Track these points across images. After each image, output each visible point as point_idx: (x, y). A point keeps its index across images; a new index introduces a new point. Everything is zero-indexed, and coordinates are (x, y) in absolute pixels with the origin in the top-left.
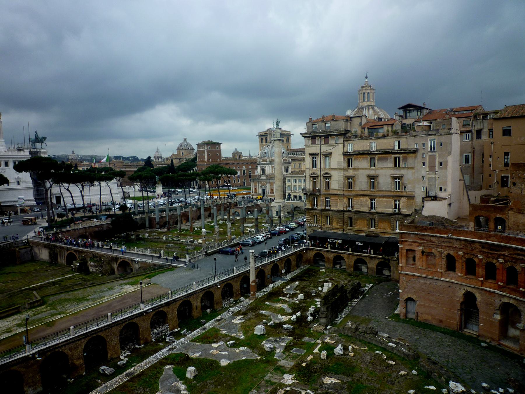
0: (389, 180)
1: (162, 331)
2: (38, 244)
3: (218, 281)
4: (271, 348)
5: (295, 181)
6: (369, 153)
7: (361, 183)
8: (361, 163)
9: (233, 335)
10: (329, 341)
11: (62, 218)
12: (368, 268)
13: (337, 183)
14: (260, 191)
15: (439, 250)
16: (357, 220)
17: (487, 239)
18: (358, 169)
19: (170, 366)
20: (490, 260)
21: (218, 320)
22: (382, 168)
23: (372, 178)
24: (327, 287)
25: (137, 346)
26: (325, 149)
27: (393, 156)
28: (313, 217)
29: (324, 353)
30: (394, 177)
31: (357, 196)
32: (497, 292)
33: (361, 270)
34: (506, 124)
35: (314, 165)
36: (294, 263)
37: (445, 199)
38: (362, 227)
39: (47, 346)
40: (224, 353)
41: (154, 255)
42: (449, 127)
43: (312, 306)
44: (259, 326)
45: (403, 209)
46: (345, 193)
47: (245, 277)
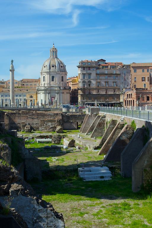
18: (101, 79)
22: (110, 79)
26: (89, 72)
31: (101, 89)
35: (84, 78)
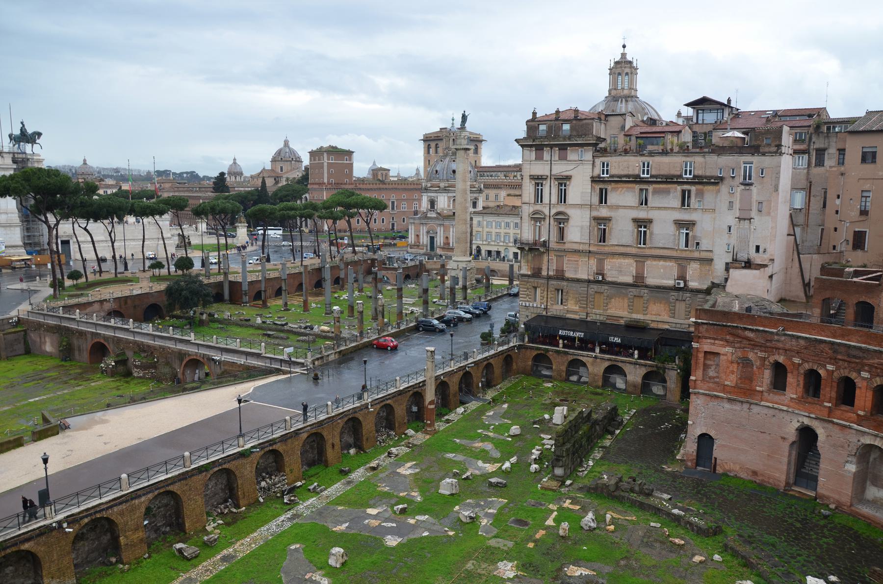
0: (671, 229)
1: (275, 484)
2: (39, 326)
3: (370, 400)
4: (471, 518)
5: (508, 225)
6: (636, 180)
7: (622, 232)
8: (624, 198)
9: (401, 494)
10: (571, 507)
11: (77, 279)
12: (626, 382)
13: (578, 231)
14: (425, 240)
15: (760, 354)
16: (611, 299)
17: (842, 337)
18: (618, 207)
19: (298, 546)
20: (845, 373)
21: (373, 469)
22: (659, 208)
23: (642, 224)
24: (559, 415)
25: (234, 510)
26: (560, 168)
27: (679, 188)
28: (533, 290)
29: (565, 525)
30: (680, 224)
31: (614, 254)
32: (855, 426)
33: (614, 386)
34: (869, 142)
35: (539, 197)
36: (497, 371)
37: (765, 266)
38: (620, 310)
39: (82, 508)
40: (390, 525)
41: (249, 350)
42: (777, 143)
43: (537, 447)
44: (448, 480)
45: (692, 281)
46: (592, 249)
47: (416, 394)
